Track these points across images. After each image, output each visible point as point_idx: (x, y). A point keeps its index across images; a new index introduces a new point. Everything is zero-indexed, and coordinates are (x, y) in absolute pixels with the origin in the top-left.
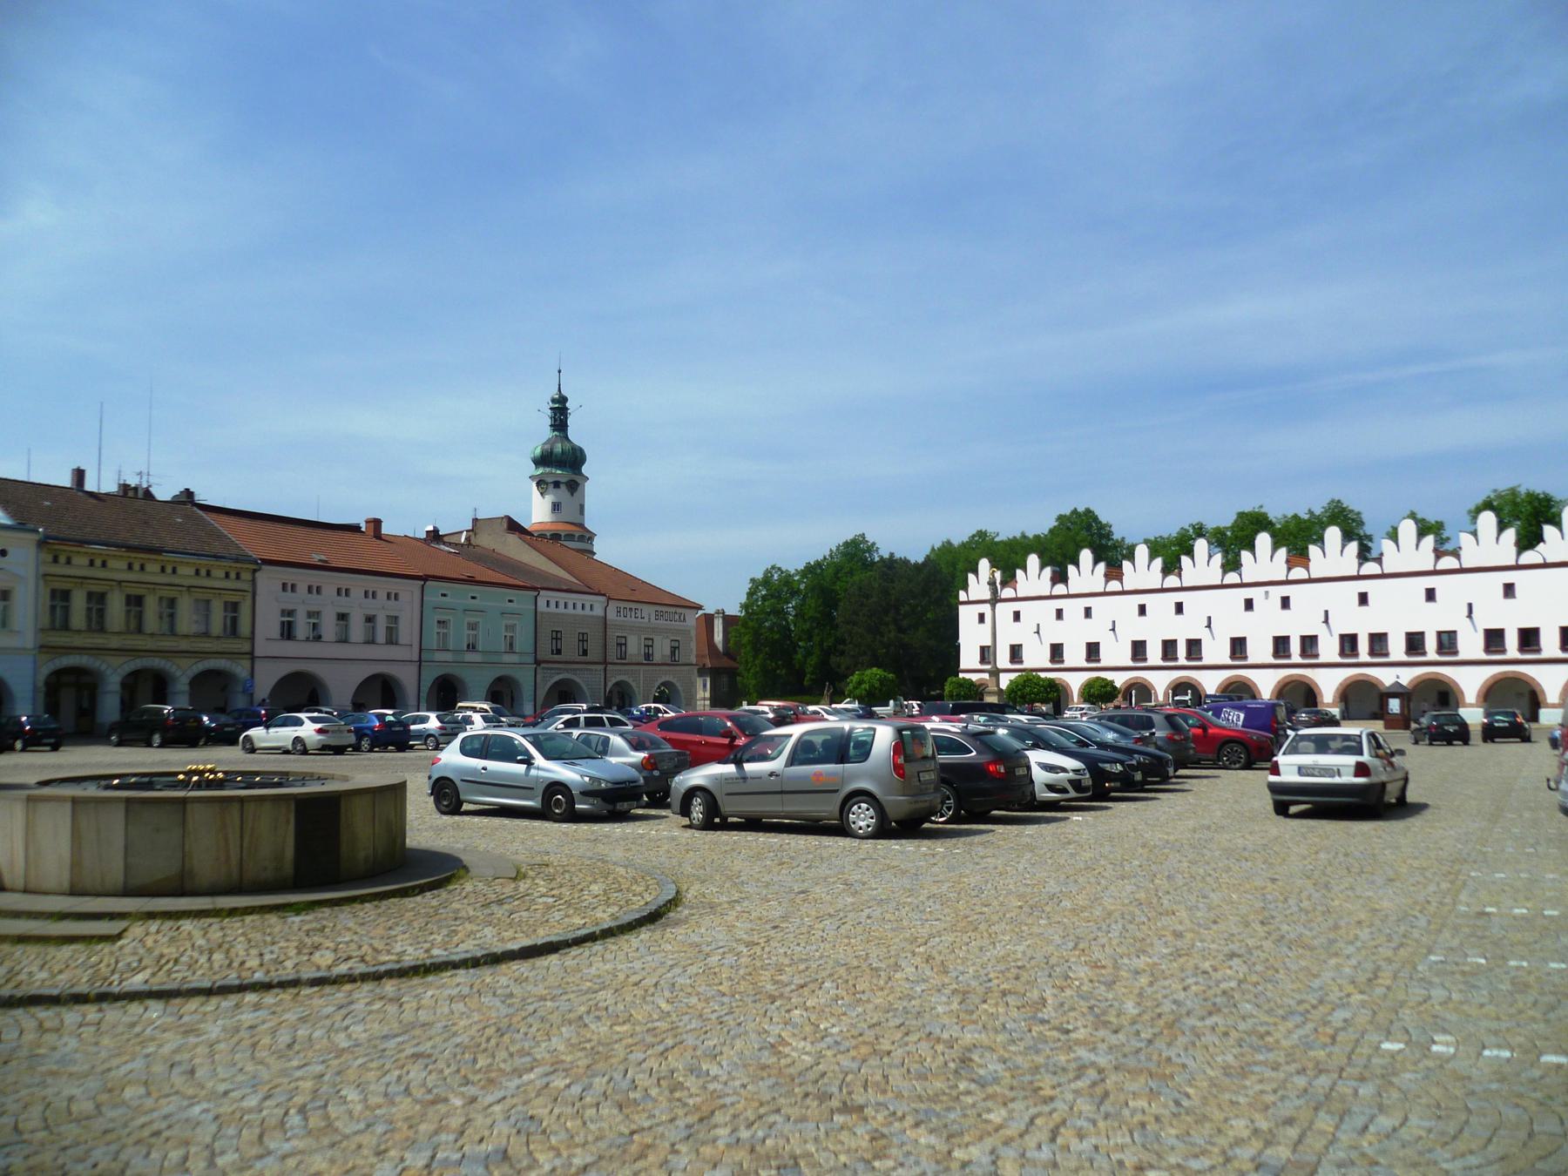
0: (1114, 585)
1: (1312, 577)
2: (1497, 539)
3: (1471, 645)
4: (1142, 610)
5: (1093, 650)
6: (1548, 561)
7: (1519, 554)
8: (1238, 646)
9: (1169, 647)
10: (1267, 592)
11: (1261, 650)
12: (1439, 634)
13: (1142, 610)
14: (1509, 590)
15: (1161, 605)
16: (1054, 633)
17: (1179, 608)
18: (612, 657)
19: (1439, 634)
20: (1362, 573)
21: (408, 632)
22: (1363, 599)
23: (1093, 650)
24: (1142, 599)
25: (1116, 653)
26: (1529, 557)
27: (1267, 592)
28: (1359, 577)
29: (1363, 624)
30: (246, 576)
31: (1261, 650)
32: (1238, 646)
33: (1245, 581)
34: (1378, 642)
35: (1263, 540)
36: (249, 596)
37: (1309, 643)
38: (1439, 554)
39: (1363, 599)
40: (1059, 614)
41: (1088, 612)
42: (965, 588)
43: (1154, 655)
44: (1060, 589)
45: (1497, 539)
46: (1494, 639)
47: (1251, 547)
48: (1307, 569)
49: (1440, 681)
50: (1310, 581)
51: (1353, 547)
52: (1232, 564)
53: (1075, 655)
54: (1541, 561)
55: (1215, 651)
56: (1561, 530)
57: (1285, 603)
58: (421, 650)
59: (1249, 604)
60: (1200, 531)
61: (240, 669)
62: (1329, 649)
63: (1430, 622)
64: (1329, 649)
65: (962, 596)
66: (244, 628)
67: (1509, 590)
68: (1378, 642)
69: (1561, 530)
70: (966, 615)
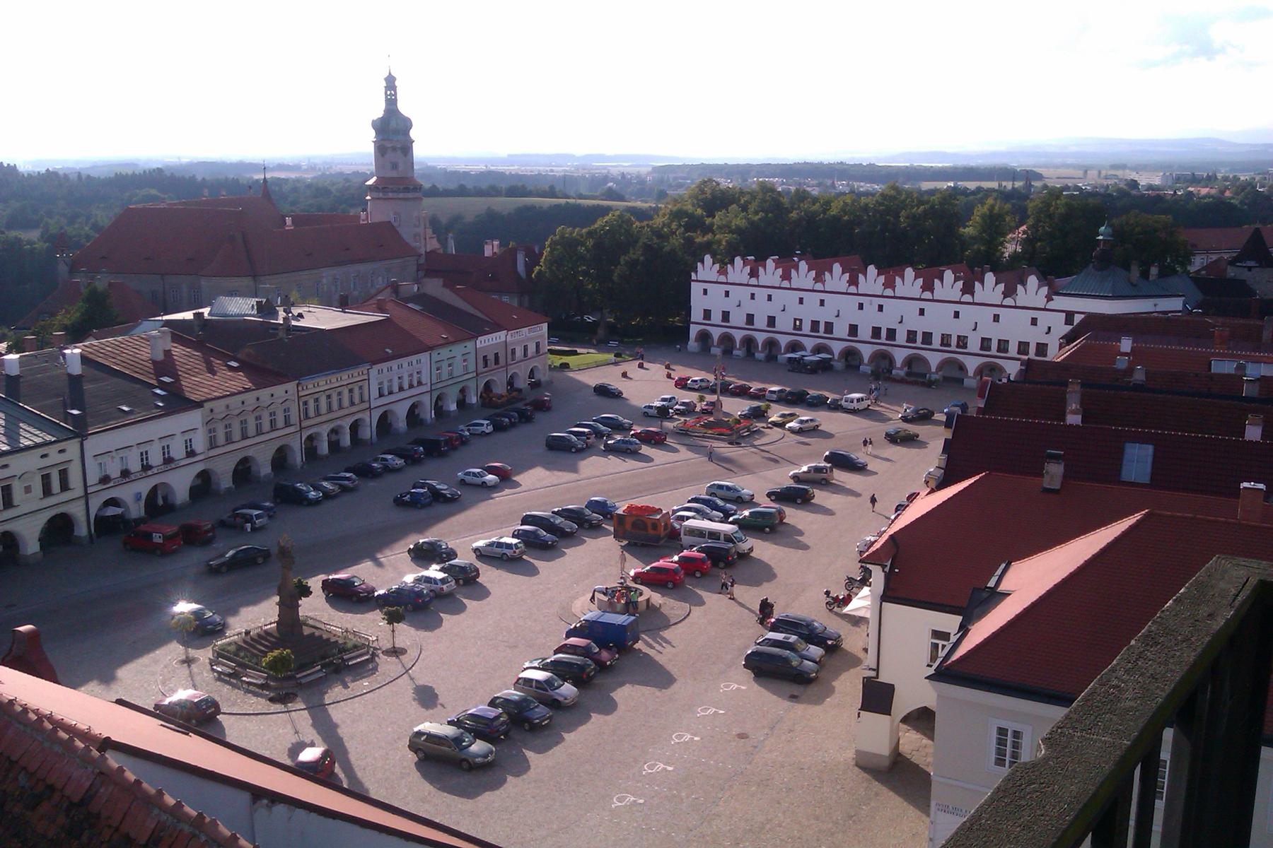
0: (786, 284)
3: (974, 345)
5: (771, 321)
8: (853, 329)
9: (815, 325)
11: (865, 333)
14: (996, 318)
16: (749, 307)
18: (510, 361)
21: (426, 379)
23: (771, 321)
24: (802, 294)
25: (784, 323)
26: (1009, 301)
29: (920, 326)
30: (365, 372)
31: (865, 333)
32: (853, 329)
34: (927, 337)
36: (367, 381)
37: (891, 333)
43: (806, 328)
44: (753, 281)
52: (853, 281)
53: (761, 322)
55: (841, 330)
57: (881, 308)
58: (431, 385)
59: (861, 306)
61: (366, 416)
62: (901, 338)
63: (955, 329)
64: (901, 338)
65: (693, 276)
66: (366, 398)
67: (996, 318)
68: (927, 337)
70: (696, 289)
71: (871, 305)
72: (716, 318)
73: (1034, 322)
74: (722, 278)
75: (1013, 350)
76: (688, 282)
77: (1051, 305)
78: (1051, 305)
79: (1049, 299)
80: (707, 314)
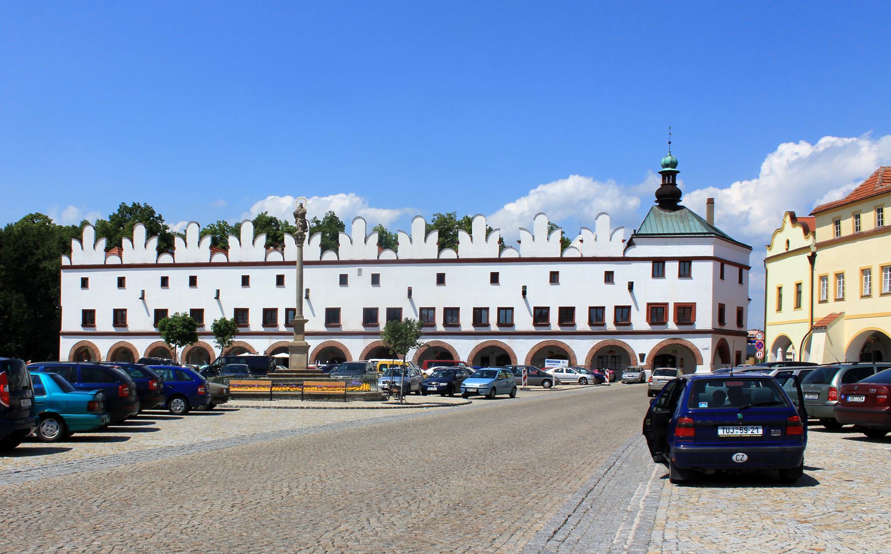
0: (220, 258)
3: (523, 321)
4: (245, 281)
8: (333, 316)
11: (352, 320)
12: (499, 309)
14: (554, 277)
15: (263, 278)
19: (499, 309)
22: (441, 279)
28: (438, 261)
31: (352, 320)
32: (333, 316)
39: (441, 279)
40: (165, 282)
41: (193, 281)
42: (68, 250)
44: (166, 258)
46: (541, 315)
50: (398, 262)
57: (375, 279)
59: (343, 280)
65: (65, 261)
67: (554, 277)
68: (452, 314)
70: (69, 281)
72: (105, 323)
73: (609, 277)
74: (113, 260)
75: (582, 322)
77: (632, 253)
79: (630, 244)
80: (88, 317)
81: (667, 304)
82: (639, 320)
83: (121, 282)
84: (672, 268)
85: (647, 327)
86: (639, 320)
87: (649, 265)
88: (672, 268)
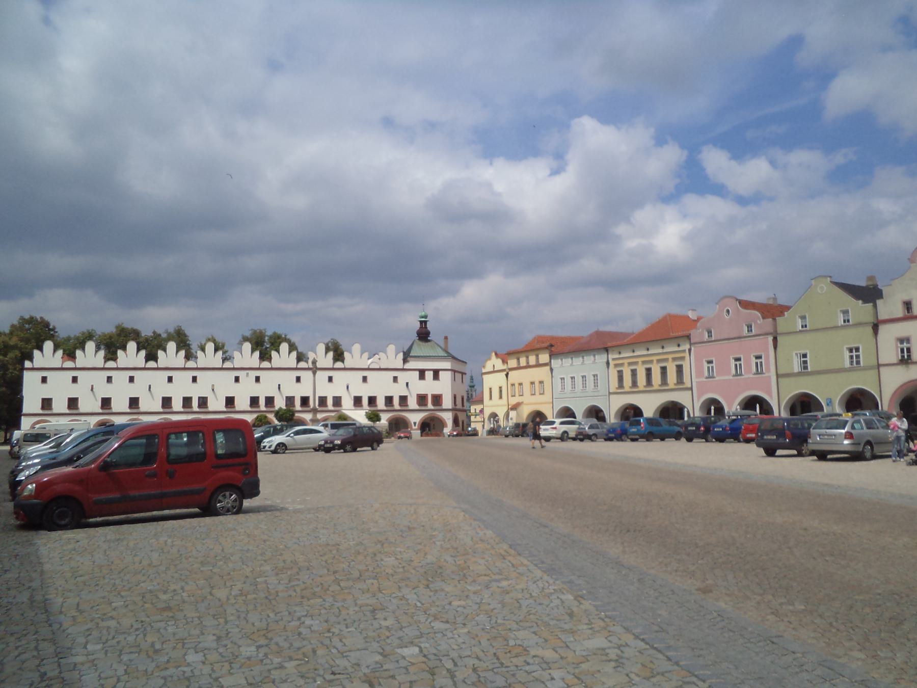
0: (152, 364)
1: (159, 366)
2: (361, 357)
5: (134, 402)
6: (381, 367)
7: (105, 362)
10: (248, 374)
13: (170, 379)
14: (365, 379)
16: (105, 391)
17: (194, 379)
20: (64, 366)
23: (134, 402)
24: (170, 373)
27: (248, 374)
28: (296, 369)
33: (78, 366)
35: (132, 346)
38: (224, 360)
40: (109, 379)
41: (131, 379)
44: (111, 364)
45: (361, 357)
47: (124, 348)
48: (270, 362)
49: (543, 414)
50: (272, 369)
51: (182, 353)
53: (120, 404)
54: (378, 367)
56: (279, 353)
59: (237, 379)
60: (90, 336)
65: (27, 364)
69: (279, 353)
71: (247, 379)
73: (395, 379)
74: (69, 364)
76: (23, 369)
77: (407, 366)
78: (407, 366)
80: (47, 403)
81: (427, 395)
82: (412, 403)
83: (75, 380)
84: (429, 375)
85: (417, 407)
86: (412, 403)
87: (417, 373)
88: (429, 375)
